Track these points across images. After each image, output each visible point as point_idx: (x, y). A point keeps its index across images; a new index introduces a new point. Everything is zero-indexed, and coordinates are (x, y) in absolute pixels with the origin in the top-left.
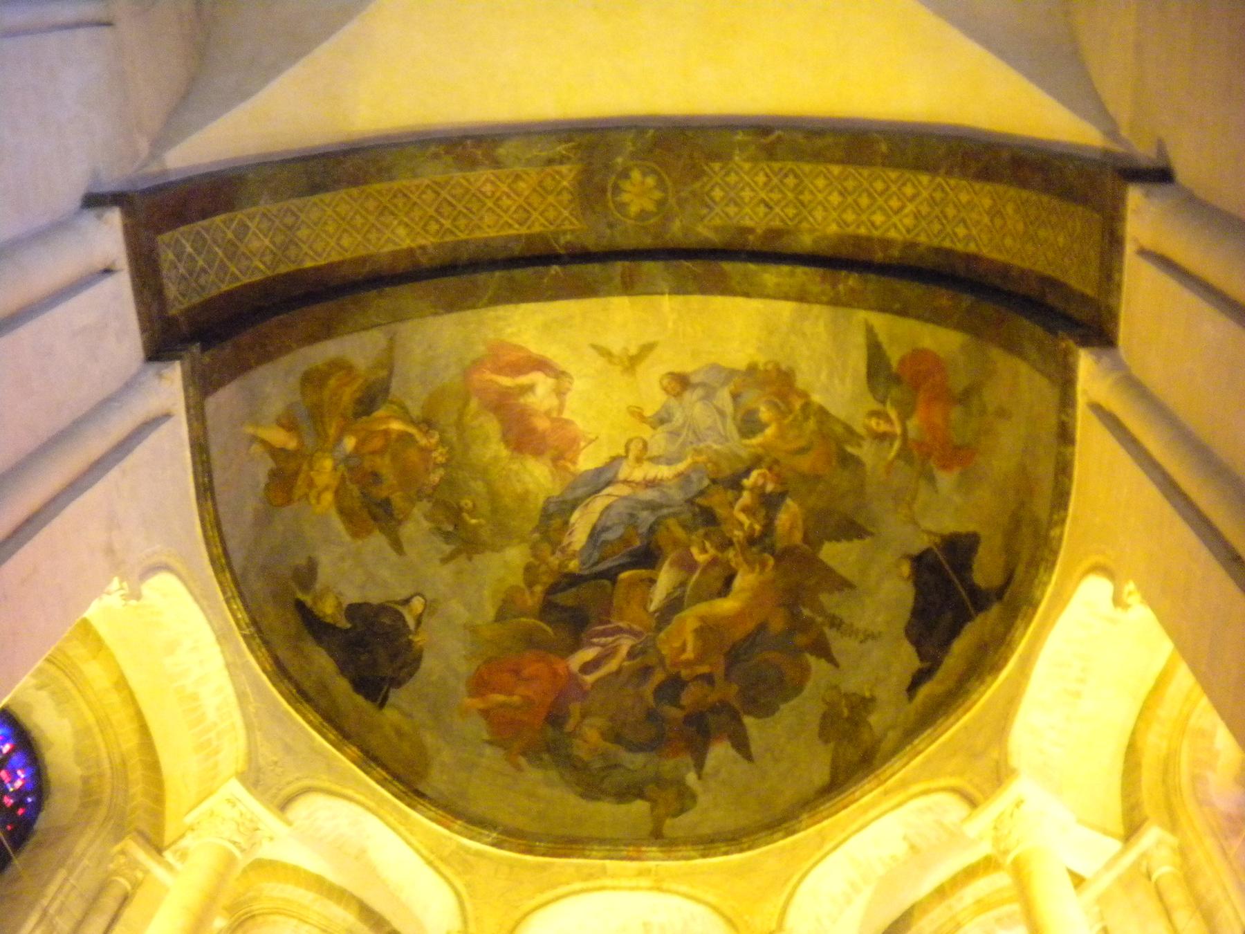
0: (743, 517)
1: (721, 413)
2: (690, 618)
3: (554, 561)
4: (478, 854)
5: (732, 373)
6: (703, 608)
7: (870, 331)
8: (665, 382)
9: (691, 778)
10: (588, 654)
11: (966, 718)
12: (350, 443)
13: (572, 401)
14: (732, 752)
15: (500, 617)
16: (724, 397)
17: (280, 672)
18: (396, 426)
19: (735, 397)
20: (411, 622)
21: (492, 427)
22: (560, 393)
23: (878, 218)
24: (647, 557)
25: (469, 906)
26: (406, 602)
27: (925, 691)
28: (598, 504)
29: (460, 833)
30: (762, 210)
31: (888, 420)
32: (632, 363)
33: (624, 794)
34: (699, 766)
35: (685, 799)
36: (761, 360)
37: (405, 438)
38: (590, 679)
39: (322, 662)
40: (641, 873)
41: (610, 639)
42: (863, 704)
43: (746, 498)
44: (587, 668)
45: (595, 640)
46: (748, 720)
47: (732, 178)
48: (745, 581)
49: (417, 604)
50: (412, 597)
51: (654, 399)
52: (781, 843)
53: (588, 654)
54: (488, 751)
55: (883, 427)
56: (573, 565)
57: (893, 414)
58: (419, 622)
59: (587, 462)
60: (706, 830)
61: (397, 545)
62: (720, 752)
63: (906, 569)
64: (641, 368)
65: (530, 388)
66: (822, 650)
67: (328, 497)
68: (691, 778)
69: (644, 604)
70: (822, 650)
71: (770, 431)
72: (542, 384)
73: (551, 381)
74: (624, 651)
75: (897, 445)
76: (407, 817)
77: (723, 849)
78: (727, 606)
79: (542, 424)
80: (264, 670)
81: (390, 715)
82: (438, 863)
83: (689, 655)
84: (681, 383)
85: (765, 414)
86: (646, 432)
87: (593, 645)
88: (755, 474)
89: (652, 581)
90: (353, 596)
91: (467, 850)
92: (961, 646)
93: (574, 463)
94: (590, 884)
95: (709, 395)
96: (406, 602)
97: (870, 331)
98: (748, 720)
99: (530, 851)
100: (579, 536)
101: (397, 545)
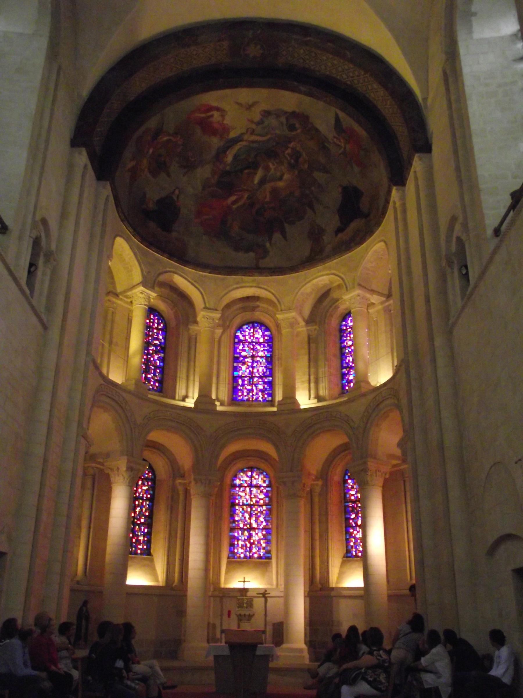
0: (287, 156)
1: (282, 123)
2: (268, 187)
3: (221, 167)
4: (205, 276)
5: (286, 113)
6: (272, 184)
7: (337, 115)
8: (262, 113)
9: (268, 245)
10: (233, 198)
11: (350, 254)
12: (151, 151)
13: (227, 117)
14: (280, 236)
15: (204, 189)
16: (283, 119)
17: (144, 240)
18: (165, 139)
19: (287, 119)
20: (175, 198)
21: (198, 130)
22: (223, 116)
23: (344, 76)
24: (254, 166)
25: (205, 297)
26: (173, 192)
27: (340, 235)
28: (237, 147)
29: (199, 271)
30: (301, 61)
31: (340, 142)
32: (249, 107)
33: (248, 250)
34: (270, 240)
35: (266, 253)
36: (297, 111)
37: (169, 141)
38: (235, 207)
39: (152, 225)
40: (254, 281)
41: (241, 193)
42: (321, 231)
43: (289, 151)
44: (234, 203)
45: (236, 193)
46: (286, 225)
47: (291, 49)
48: (286, 177)
49: (177, 192)
50: (175, 190)
51: (257, 117)
52: (294, 274)
53: (233, 198)
54: (204, 237)
55: (338, 143)
56: (228, 168)
57: (342, 141)
58: (178, 197)
59: (232, 135)
60: (272, 265)
61: (169, 175)
62: (277, 236)
63: (340, 190)
64: (253, 109)
65: (212, 116)
66: (311, 207)
67: (146, 170)
68: (268, 245)
69: (252, 181)
70: (311, 207)
71: (299, 131)
72: (216, 114)
73: (219, 113)
74: (246, 196)
75: (342, 150)
76: (183, 269)
77: (278, 274)
78: (281, 184)
79: (216, 126)
80: (139, 241)
81: (174, 234)
82: (195, 283)
83: (268, 199)
84: (267, 113)
85: (297, 126)
86: (254, 126)
87: (235, 195)
88: (293, 143)
89: (256, 174)
90: (156, 198)
91: (202, 276)
92: (353, 225)
93: (228, 136)
94: (238, 286)
95: (278, 116)
96: (173, 192)
97: (337, 115)
98: (286, 225)
99: (220, 274)
100: (229, 158)
101: (169, 175)
